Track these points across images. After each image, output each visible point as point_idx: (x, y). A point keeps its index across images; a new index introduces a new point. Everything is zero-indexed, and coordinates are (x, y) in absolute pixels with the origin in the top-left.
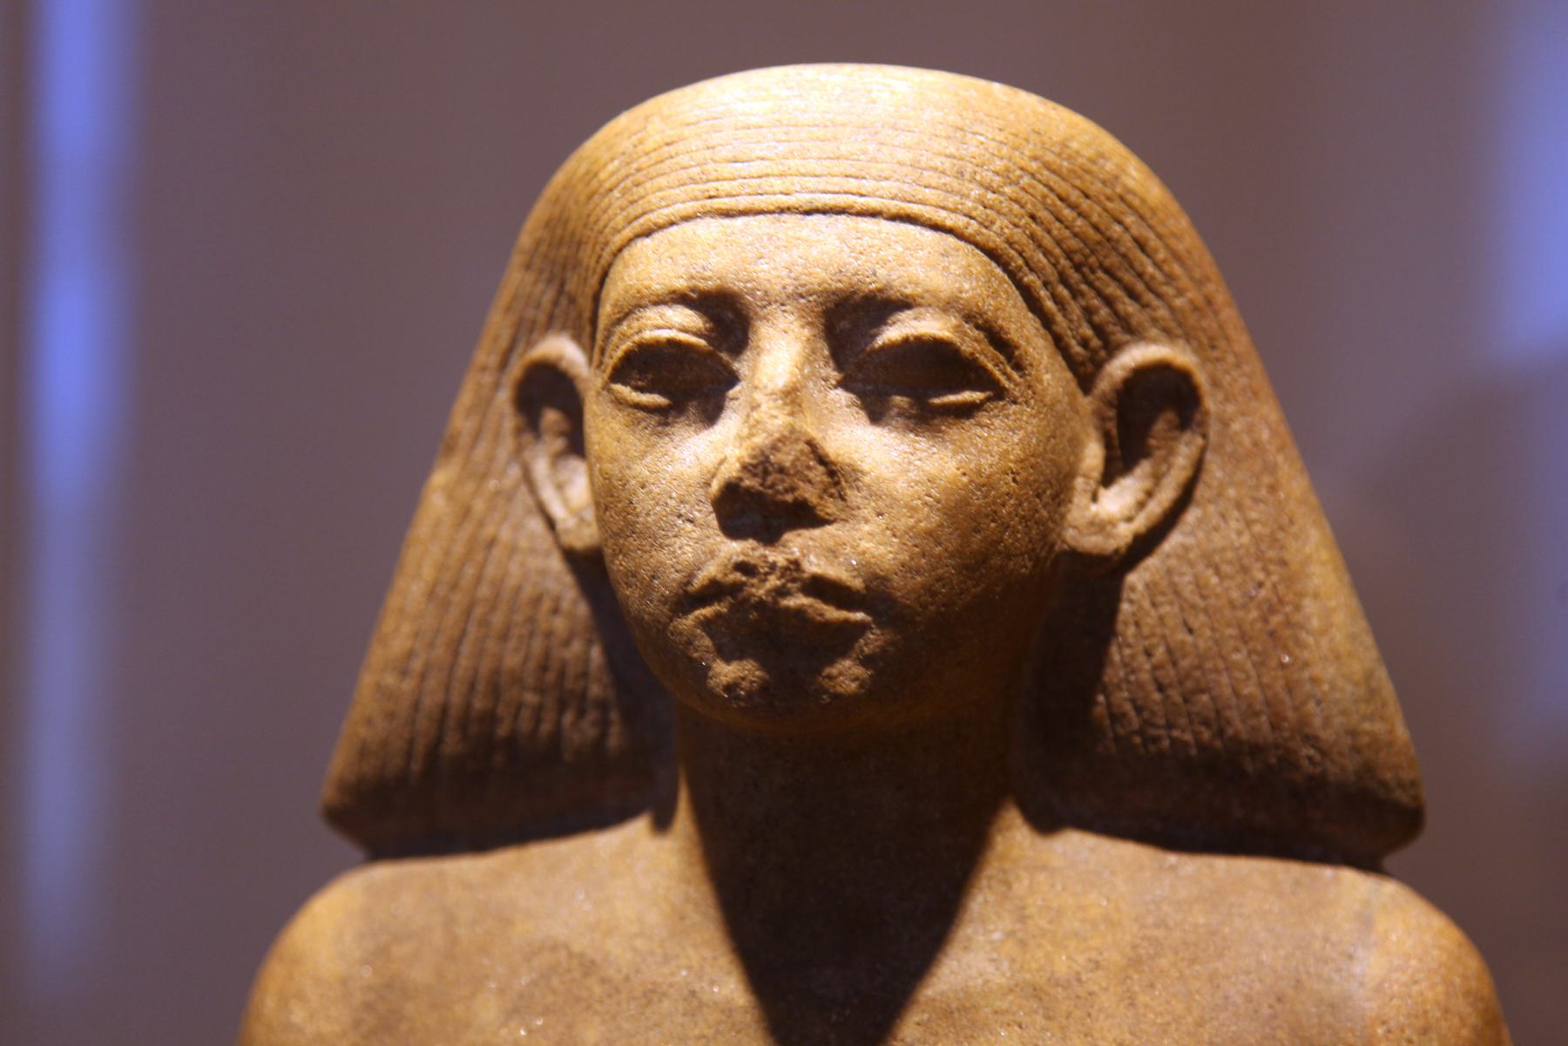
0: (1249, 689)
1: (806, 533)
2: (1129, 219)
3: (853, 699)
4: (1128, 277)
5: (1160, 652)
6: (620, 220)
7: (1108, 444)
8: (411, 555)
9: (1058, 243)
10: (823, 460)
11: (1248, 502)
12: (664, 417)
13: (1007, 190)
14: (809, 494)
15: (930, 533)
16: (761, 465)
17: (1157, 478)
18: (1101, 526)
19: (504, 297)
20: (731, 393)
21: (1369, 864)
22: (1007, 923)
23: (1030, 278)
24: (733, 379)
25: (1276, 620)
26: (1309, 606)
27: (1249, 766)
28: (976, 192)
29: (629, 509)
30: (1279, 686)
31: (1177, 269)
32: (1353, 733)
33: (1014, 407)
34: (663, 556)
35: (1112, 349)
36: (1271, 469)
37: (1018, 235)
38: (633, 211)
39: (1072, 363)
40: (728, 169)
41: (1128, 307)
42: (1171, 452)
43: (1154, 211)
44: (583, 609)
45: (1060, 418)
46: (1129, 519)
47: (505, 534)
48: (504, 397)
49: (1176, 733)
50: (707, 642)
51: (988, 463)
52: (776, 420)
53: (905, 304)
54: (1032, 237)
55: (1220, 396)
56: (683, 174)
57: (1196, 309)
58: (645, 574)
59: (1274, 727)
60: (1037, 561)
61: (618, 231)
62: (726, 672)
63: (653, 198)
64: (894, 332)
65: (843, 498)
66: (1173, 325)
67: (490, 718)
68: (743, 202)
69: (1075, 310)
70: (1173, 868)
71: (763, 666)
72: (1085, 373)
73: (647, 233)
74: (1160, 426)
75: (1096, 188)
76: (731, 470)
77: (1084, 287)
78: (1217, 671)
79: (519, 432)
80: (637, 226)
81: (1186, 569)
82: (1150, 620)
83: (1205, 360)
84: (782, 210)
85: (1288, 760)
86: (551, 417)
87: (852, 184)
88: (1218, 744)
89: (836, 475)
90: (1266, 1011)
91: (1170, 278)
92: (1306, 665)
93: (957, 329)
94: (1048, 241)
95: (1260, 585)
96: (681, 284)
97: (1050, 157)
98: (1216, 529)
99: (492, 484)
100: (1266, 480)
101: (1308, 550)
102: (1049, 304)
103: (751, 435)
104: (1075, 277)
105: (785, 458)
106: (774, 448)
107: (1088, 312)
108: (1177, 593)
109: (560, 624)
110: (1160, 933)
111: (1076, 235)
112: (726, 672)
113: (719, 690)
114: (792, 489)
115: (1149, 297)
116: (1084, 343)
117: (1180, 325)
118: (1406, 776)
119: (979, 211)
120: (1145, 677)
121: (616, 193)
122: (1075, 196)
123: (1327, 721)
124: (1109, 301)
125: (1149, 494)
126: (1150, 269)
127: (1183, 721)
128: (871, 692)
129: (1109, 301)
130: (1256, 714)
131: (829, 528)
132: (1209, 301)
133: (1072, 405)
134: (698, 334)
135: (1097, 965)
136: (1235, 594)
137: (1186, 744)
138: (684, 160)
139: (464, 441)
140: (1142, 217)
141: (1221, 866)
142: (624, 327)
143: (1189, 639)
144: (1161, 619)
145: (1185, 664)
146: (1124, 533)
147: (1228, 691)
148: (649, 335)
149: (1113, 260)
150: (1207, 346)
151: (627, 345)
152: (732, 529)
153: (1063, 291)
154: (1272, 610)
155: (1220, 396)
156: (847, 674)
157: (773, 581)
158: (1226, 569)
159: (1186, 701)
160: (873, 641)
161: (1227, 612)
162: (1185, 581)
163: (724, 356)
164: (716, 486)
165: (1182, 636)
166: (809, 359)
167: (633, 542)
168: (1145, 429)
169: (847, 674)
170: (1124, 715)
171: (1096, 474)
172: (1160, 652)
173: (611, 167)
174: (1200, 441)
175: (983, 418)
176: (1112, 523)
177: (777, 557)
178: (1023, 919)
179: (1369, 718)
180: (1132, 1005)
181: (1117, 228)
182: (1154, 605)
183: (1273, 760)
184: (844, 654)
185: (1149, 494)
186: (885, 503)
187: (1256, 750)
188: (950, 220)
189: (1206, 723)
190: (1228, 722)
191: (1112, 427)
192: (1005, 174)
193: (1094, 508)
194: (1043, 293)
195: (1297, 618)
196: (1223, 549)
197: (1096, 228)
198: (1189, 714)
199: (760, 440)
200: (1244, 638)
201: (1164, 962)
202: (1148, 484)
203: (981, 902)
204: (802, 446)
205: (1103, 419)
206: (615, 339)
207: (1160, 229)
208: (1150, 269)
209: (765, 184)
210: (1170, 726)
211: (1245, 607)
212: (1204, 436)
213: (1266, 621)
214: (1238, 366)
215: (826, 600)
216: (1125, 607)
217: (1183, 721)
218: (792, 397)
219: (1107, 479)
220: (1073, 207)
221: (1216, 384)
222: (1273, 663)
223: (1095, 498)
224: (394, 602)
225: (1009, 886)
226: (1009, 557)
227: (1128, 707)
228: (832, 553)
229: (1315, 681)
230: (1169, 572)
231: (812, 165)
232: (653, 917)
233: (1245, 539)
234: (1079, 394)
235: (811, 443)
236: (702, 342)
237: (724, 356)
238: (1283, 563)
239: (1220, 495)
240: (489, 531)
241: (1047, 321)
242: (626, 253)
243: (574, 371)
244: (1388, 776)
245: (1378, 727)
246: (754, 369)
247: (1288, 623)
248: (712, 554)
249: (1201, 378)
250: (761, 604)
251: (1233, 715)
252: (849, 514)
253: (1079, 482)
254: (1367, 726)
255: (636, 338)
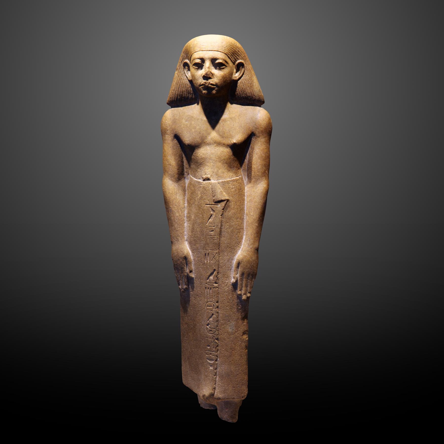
0: (249, 91)
1: (210, 79)
2: (238, 49)
3: (215, 94)
4: (237, 54)
5: (241, 88)
6: (193, 51)
7: (236, 70)
8: (174, 80)
9: (231, 52)
10: (211, 73)
11: (249, 74)
12: (198, 69)
13: (226, 48)
14: (210, 76)
15: (221, 79)
16: (206, 74)
17: (241, 72)
18: (236, 77)
19: (181, 56)
20: (204, 67)
21: (260, 106)
22: (228, 112)
23: (229, 56)
24: (203, 66)
25: (251, 85)
26: (254, 83)
27: (249, 98)
28: (224, 48)
29: (195, 77)
30: (252, 91)
31: (242, 53)
32: (258, 95)
33: (227, 68)
34: (198, 81)
35: (236, 61)
36: (251, 71)
37: (228, 52)
38: (194, 50)
39: (233, 63)
40: (202, 46)
41: (238, 57)
42: (242, 70)
43: (240, 48)
44: (190, 85)
45: (232, 68)
46: (238, 76)
47: (183, 78)
48: (182, 65)
49: (243, 95)
50: (202, 89)
51: (226, 73)
52: (207, 70)
53: (218, 59)
54: (229, 52)
55: (246, 64)
56: (198, 47)
57: (244, 57)
58: (197, 83)
59: (251, 95)
60: (230, 81)
61: (192, 52)
62: (204, 92)
63: (196, 49)
64: (217, 62)
65: (213, 76)
66: (242, 58)
67: (182, 95)
68: (204, 50)
69: (233, 58)
70: (243, 107)
71: (207, 91)
72: (234, 63)
73: (195, 52)
74: (241, 68)
75: (234, 46)
76: (204, 74)
77: (234, 56)
78: (246, 90)
79: (183, 69)
80: (194, 51)
81: (243, 81)
82: (240, 85)
83: (245, 61)
84: (207, 50)
85: (252, 97)
86: (186, 67)
87: (213, 48)
88: (246, 96)
89: (213, 74)
90: (250, 119)
91: (241, 54)
92: (254, 89)
93: (223, 61)
94: (230, 52)
95: (250, 82)
96: (199, 57)
97: (230, 44)
98: (246, 77)
99: (181, 73)
100: (250, 72)
101: (254, 78)
102: (231, 58)
103: (205, 71)
104: (233, 55)
105: (208, 73)
106: (207, 72)
107: (234, 58)
108: (242, 83)
109: (188, 86)
110: (241, 113)
111: (233, 51)
112: (204, 92)
113: (203, 93)
114: (209, 76)
115: (240, 56)
116: (234, 61)
117: (242, 58)
118: (263, 98)
119: (224, 50)
120: (240, 90)
121: (192, 48)
122: (232, 47)
123: (256, 94)
124: (236, 57)
125: (240, 74)
126: (239, 53)
127: (243, 94)
128: (216, 93)
129: (236, 57)
130: (250, 93)
131: (212, 79)
132: (245, 56)
133: (233, 67)
134: (200, 62)
135: (236, 116)
136: (248, 83)
137: (244, 96)
138: (198, 45)
139: (178, 69)
140: (239, 49)
141: (247, 107)
142: (194, 61)
143: (244, 87)
144: (241, 85)
145: (243, 89)
146: (238, 78)
147: (247, 91)
148: (196, 62)
149: (236, 53)
150: (245, 60)
151: (193, 63)
152: (204, 79)
153: (232, 56)
154: (251, 84)
155: (246, 64)
156: (214, 92)
157: (208, 84)
158: (247, 80)
159: (243, 92)
160: (216, 89)
161: (247, 84)
162: (243, 82)
163: (203, 64)
164: (202, 75)
165: (243, 87)
166: (210, 64)
167: (195, 80)
168: (239, 68)
169: (214, 92)
170: (238, 94)
171: (235, 72)
172: (241, 88)
173: (192, 45)
174: (244, 69)
175: (225, 69)
176: (237, 77)
177: (208, 82)
178: (230, 112)
179: (260, 93)
180: (239, 119)
181: (236, 50)
182: (241, 84)
183: (251, 97)
184: (214, 90)
185: (240, 74)
186: (217, 77)
187: (250, 97)
188: (222, 51)
189: (245, 94)
190: (247, 94)
191: (237, 68)
192: (226, 46)
193: (235, 75)
194: (230, 57)
195: (253, 85)
196: (246, 79)
197: (235, 50)
198: (244, 94)
199: (206, 72)
200: (248, 87)
201: (242, 115)
202: (240, 73)
203: (226, 111)
204: (210, 72)
205: (236, 67)
206: (193, 62)
207: (240, 50)
208: (239, 53)
209: (206, 48)
210: (242, 95)
211: (249, 84)
212: (245, 68)
213: (250, 85)
214: (248, 62)
215: (212, 85)
216: (238, 84)
217: (243, 94)
218: (209, 68)
219: (236, 73)
220: (232, 48)
221: (246, 63)
222: (251, 89)
223: (235, 74)
224: (173, 84)
225: (228, 109)
226: (228, 81)
227: (239, 93)
228: (213, 81)
229: (255, 90)
230: (242, 81)
231: (209, 46)
232: (198, 113)
233: (248, 78)
234: (234, 65)
235: (210, 72)
236: (201, 62)
237: (203, 64)
238: (252, 80)
239: (246, 74)
240: (181, 78)
241: (230, 59)
242: (193, 54)
243: (188, 63)
244: (261, 98)
245: (260, 94)
246: (205, 65)
247: (252, 85)
248: (202, 81)
249: (244, 63)
250: (207, 86)
251: (248, 93)
252: (214, 78)
253: (234, 73)
254: (259, 94)
255: (195, 62)
